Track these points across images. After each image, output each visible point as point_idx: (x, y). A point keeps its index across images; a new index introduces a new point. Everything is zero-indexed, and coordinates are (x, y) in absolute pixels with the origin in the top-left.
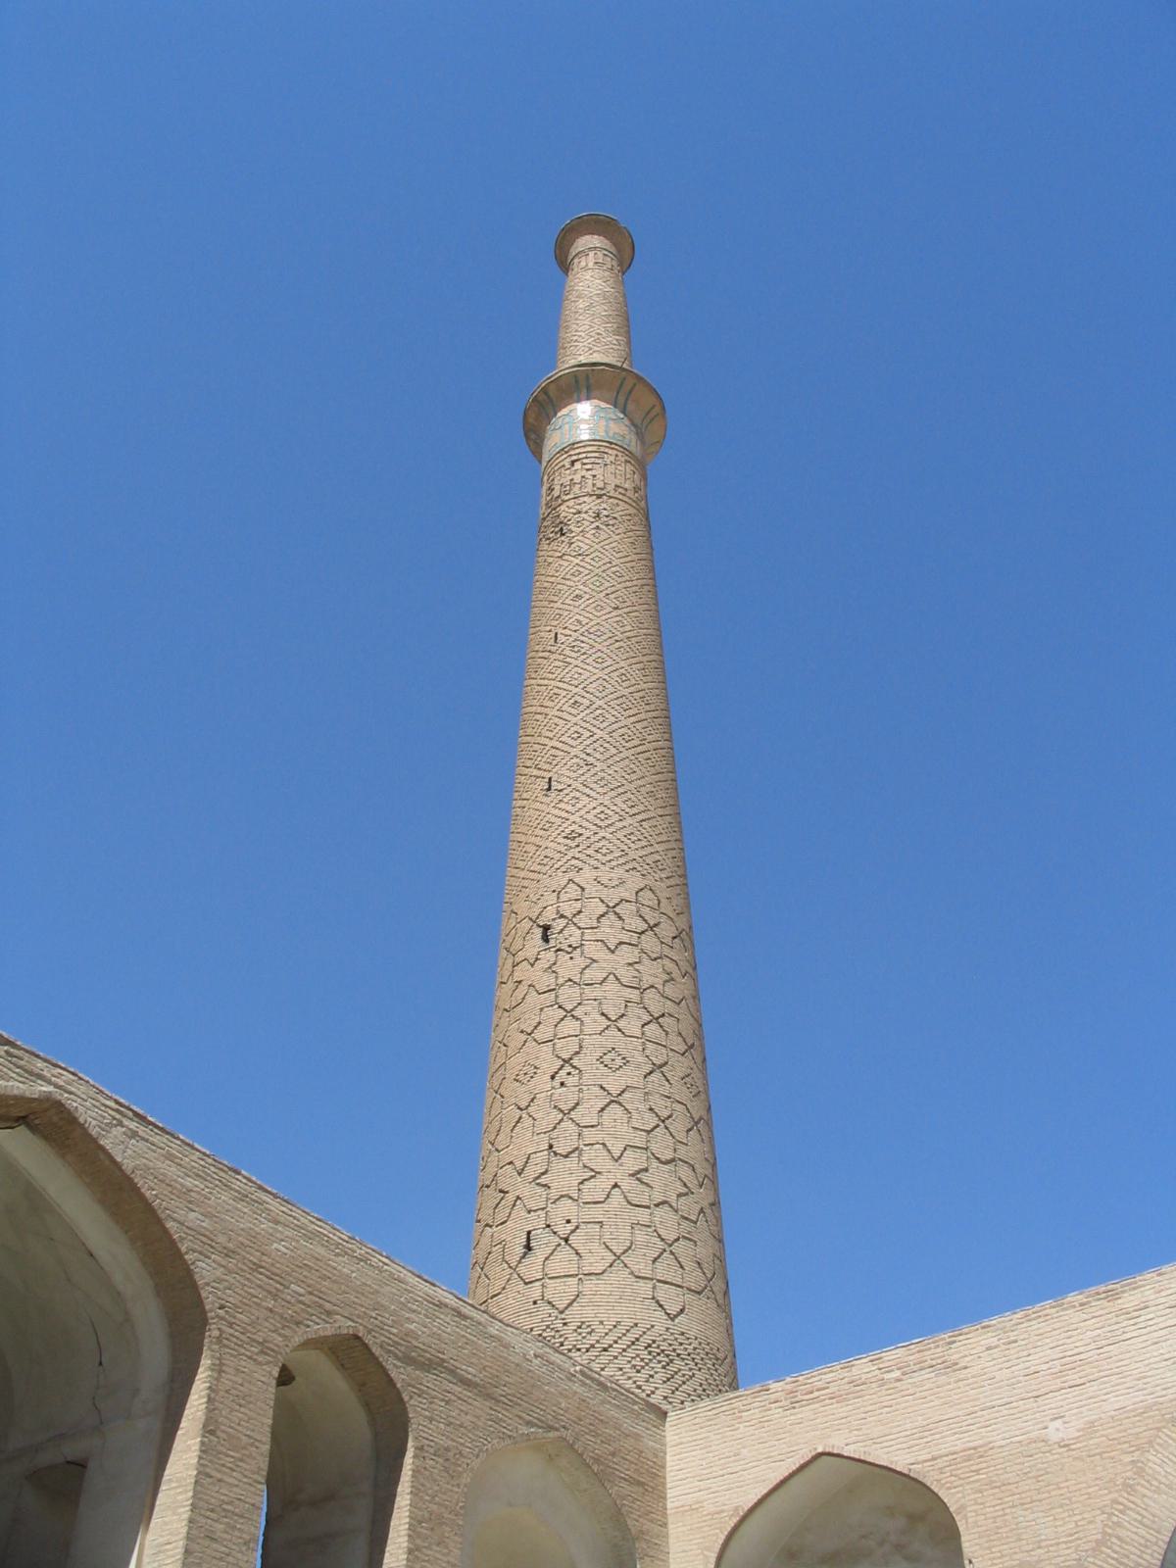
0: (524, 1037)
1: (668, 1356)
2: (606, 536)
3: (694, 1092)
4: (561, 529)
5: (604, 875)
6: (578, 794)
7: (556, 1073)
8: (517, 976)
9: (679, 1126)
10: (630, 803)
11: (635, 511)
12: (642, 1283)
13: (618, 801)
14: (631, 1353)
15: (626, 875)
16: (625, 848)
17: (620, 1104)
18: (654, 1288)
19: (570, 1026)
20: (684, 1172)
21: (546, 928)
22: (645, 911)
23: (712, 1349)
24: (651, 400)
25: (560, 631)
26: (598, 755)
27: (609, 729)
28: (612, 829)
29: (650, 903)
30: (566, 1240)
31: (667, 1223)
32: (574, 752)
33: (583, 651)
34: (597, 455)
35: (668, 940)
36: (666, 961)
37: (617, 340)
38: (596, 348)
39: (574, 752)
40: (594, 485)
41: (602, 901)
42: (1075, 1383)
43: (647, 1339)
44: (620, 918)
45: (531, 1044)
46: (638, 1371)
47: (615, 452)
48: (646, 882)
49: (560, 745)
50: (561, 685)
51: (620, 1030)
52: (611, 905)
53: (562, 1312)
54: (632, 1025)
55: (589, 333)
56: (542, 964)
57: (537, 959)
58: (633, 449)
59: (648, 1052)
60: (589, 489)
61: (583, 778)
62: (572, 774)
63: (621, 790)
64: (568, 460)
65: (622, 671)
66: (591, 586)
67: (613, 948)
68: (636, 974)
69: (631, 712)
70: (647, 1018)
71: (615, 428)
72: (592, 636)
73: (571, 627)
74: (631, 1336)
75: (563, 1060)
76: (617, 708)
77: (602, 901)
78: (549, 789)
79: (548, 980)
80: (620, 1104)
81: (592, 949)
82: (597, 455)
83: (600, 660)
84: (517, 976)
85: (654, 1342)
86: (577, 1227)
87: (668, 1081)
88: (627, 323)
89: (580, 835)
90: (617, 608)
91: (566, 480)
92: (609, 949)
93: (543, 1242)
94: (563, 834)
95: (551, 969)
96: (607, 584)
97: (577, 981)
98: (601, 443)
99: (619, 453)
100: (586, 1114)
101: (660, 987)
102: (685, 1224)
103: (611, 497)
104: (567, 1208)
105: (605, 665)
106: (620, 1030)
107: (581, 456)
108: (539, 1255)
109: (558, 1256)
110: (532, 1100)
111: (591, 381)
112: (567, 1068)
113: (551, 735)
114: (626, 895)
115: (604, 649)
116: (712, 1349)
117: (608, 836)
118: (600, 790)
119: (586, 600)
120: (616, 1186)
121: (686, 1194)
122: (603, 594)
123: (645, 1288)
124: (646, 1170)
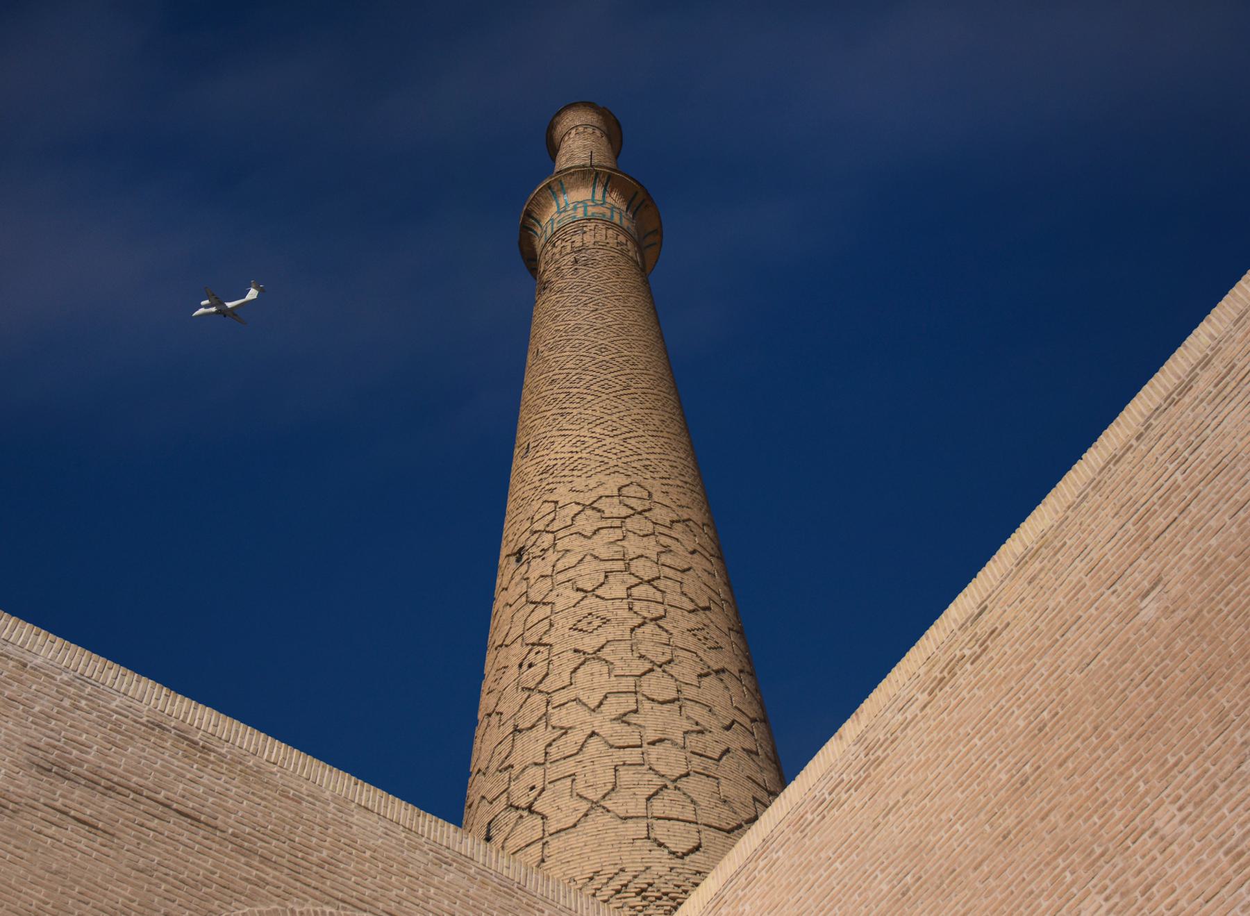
1: (674, 899)
5: (579, 483)
12: (630, 823)
29: (639, 495)
43: (641, 882)
44: (599, 511)
59: (636, 609)
74: (616, 884)
85: (650, 885)
102: (696, 760)
120: (593, 734)
124: (636, 711)
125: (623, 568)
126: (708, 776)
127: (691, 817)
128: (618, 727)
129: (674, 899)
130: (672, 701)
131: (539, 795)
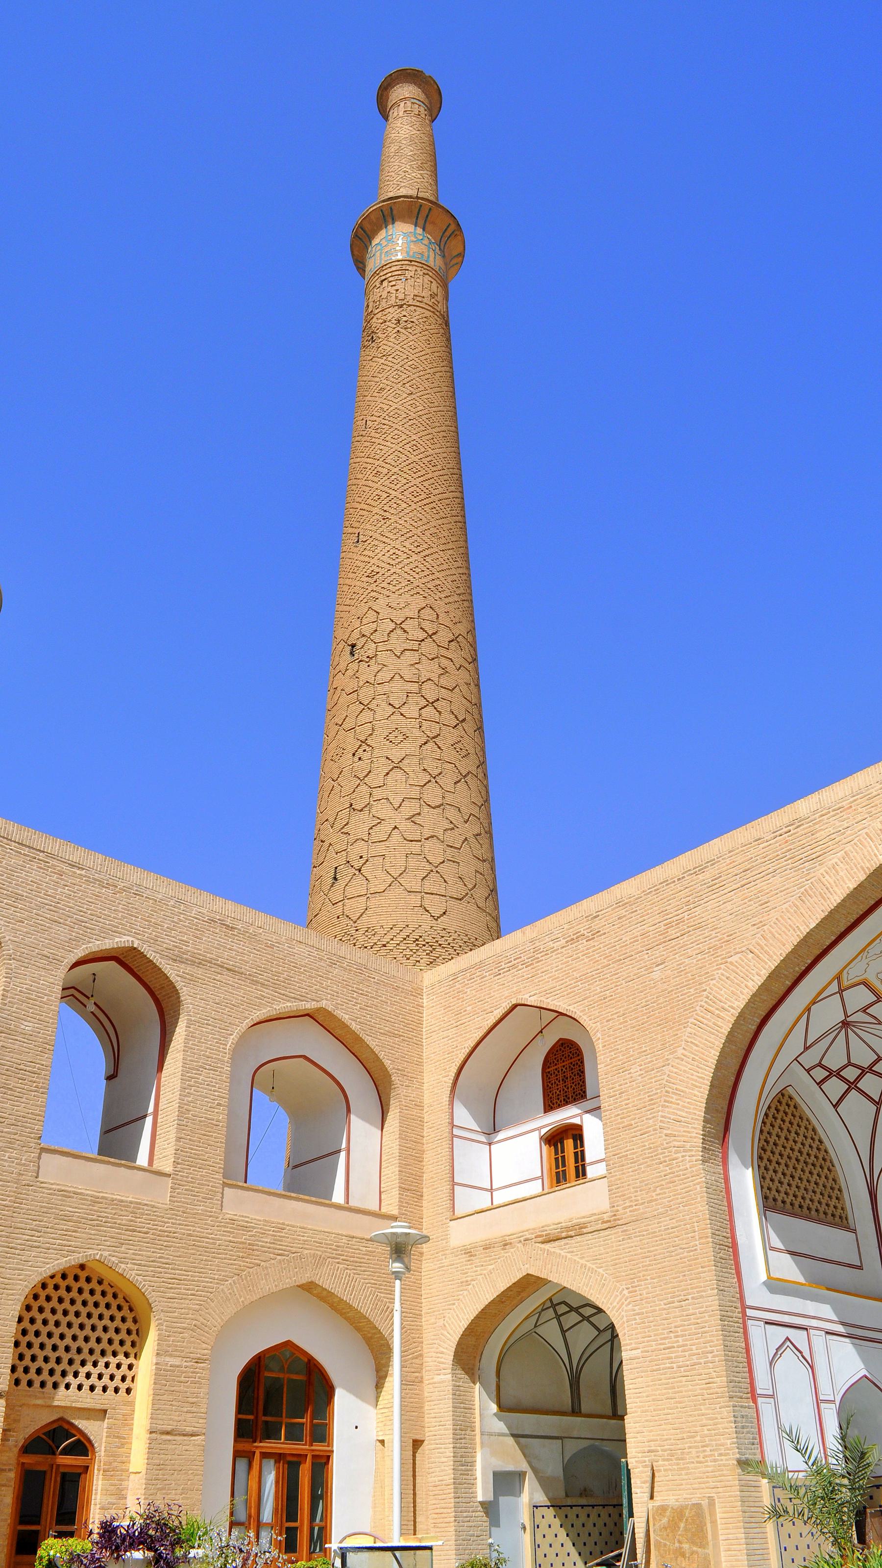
0: (337, 727)
1: (431, 946)
2: (405, 337)
3: (464, 753)
5: (394, 600)
6: (376, 543)
9: (447, 781)
10: (416, 544)
11: (431, 314)
12: (413, 895)
13: (407, 544)
14: (403, 946)
15: (411, 599)
18: (422, 898)
19: (367, 716)
20: (451, 813)
21: (353, 646)
22: (427, 625)
23: (469, 939)
24: (448, 220)
25: (369, 418)
26: (392, 511)
27: (401, 490)
28: (401, 565)
29: (430, 618)
31: (435, 851)
32: (375, 510)
33: (384, 431)
34: (400, 273)
36: (443, 660)
37: (421, 174)
38: (403, 184)
39: (375, 510)
40: (396, 297)
42: (673, 937)
43: (415, 935)
45: (342, 732)
46: (408, 959)
47: (415, 268)
48: (427, 602)
51: (402, 714)
52: (398, 622)
53: (355, 922)
54: (411, 710)
55: (403, 172)
56: (350, 673)
57: (347, 670)
58: (432, 264)
59: (423, 728)
60: (392, 301)
62: (374, 528)
63: (408, 535)
64: (379, 280)
65: (414, 442)
66: (392, 379)
68: (416, 672)
69: (419, 474)
70: (424, 703)
71: (415, 248)
72: (391, 419)
73: (376, 414)
74: (404, 934)
76: (408, 472)
79: (352, 685)
81: (382, 657)
82: (400, 273)
83: (396, 437)
85: (421, 937)
87: (439, 748)
88: (433, 161)
91: (376, 298)
93: (346, 873)
94: (366, 574)
95: (356, 676)
96: (404, 376)
97: (373, 682)
98: (403, 262)
99: (419, 269)
100: (375, 779)
101: (436, 680)
102: (449, 850)
103: (409, 305)
104: (360, 848)
105: (400, 440)
106: (402, 714)
107: (387, 276)
108: (341, 883)
109: (353, 882)
111: (395, 212)
113: (360, 500)
114: (411, 615)
115: (400, 428)
116: (469, 939)
117: (398, 571)
118: (394, 537)
119: (396, 390)
120: (396, 827)
121: (453, 829)
123: (415, 899)
124: (419, 814)
125: (417, 691)
126: (454, 862)
127: (443, 892)
128: (410, 824)
129: (431, 946)
130: (439, 806)
131: (365, 863)
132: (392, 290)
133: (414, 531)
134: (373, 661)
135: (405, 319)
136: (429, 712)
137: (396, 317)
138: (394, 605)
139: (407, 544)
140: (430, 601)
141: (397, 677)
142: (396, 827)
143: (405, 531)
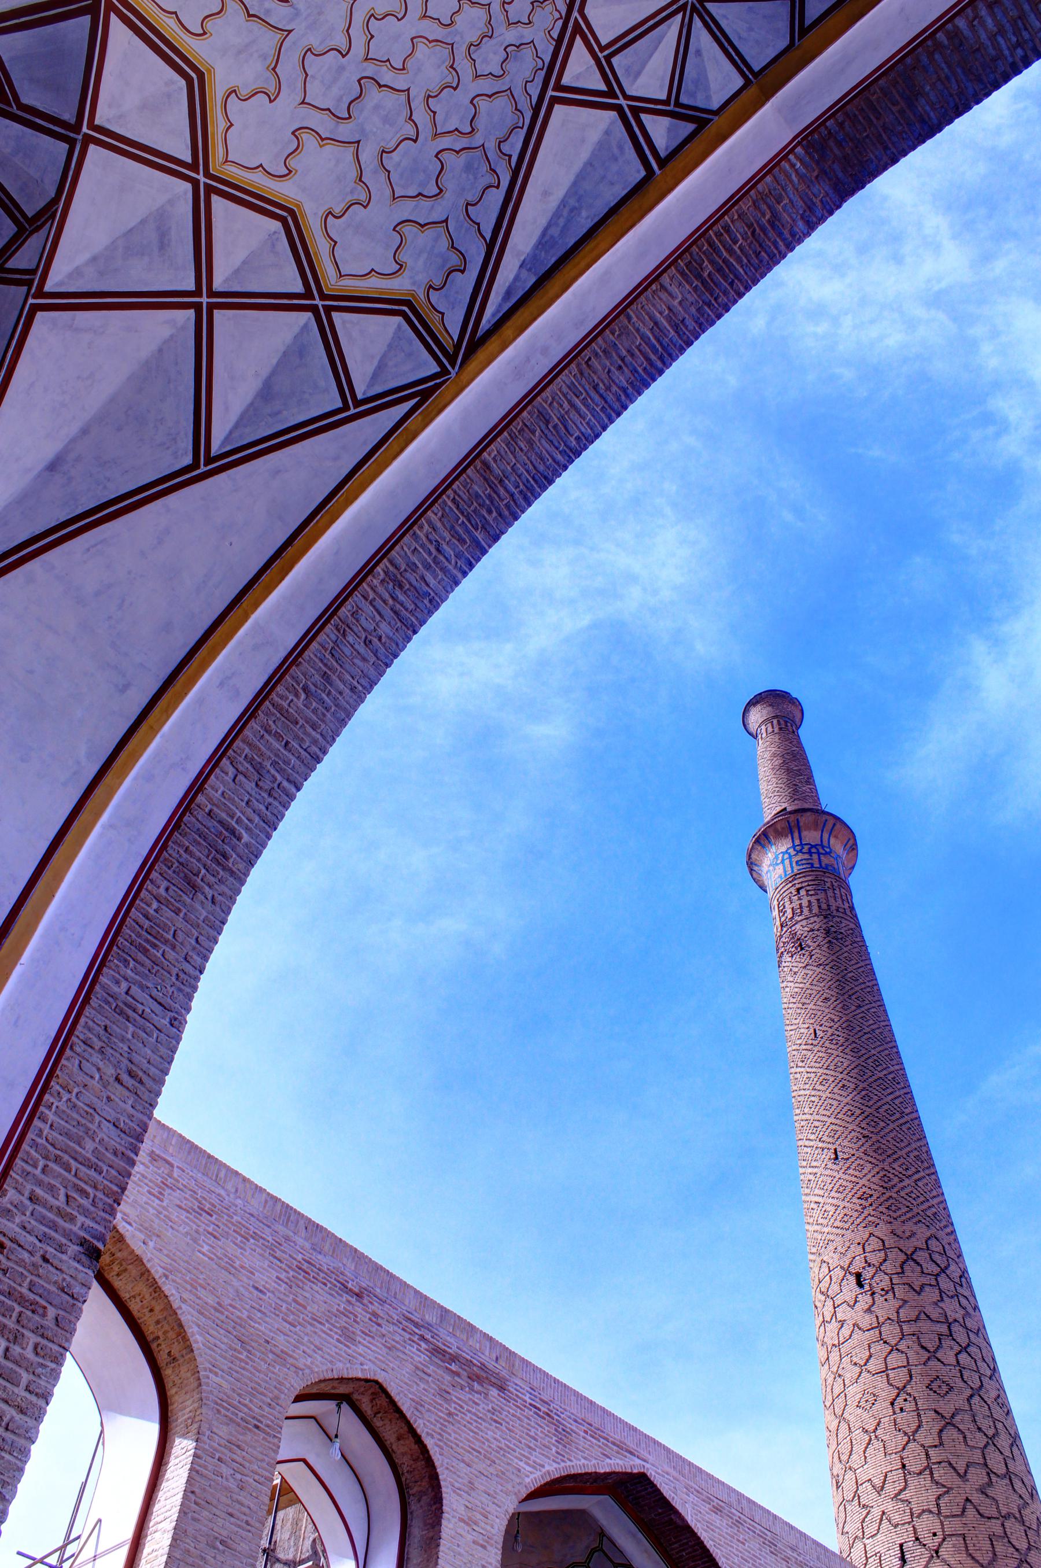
0: (857, 1369)
4: (800, 945)
6: (862, 1162)
7: (895, 1400)
8: (840, 1316)
10: (904, 1167)
13: (895, 1165)
16: (909, 1204)
17: (954, 1425)
25: (817, 1028)
28: (896, 1189)
30: (937, 1552)
33: (840, 1043)
35: (957, 1280)
36: (962, 1299)
41: (901, 1250)
49: (838, 1122)
50: (828, 1072)
51: (939, 1360)
52: (909, 1253)
57: (856, 1302)
61: (864, 1148)
63: (895, 1156)
67: (918, 1289)
69: (889, 1091)
75: (898, 1388)
77: (901, 1250)
78: (836, 1158)
80: (954, 1425)
84: (840, 1316)
86: (944, 1540)
89: (871, 1196)
90: (859, 1006)
92: (914, 1290)
101: (961, 1320)
110: (878, 1424)
111: (801, 824)
112: (903, 1396)
113: (828, 1113)
117: (895, 1195)
118: (880, 1158)
120: (967, 1500)
122: (846, 996)
128: (982, 1497)
132: (813, 899)
133: (900, 1153)
134: (890, 1295)
135: (833, 929)
136: (963, 1357)
137: (824, 926)
138: (899, 1233)
139: (895, 1165)
140: (933, 1231)
141: (923, 1316)
142: (967, 1500)
143: (891, 1152)
